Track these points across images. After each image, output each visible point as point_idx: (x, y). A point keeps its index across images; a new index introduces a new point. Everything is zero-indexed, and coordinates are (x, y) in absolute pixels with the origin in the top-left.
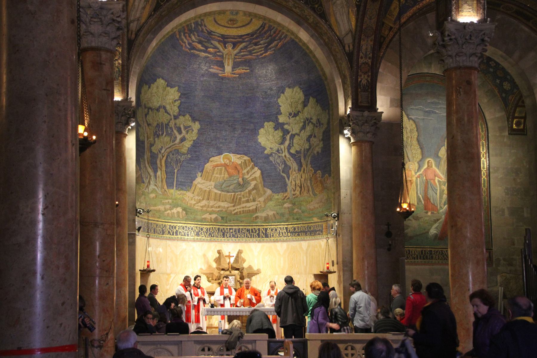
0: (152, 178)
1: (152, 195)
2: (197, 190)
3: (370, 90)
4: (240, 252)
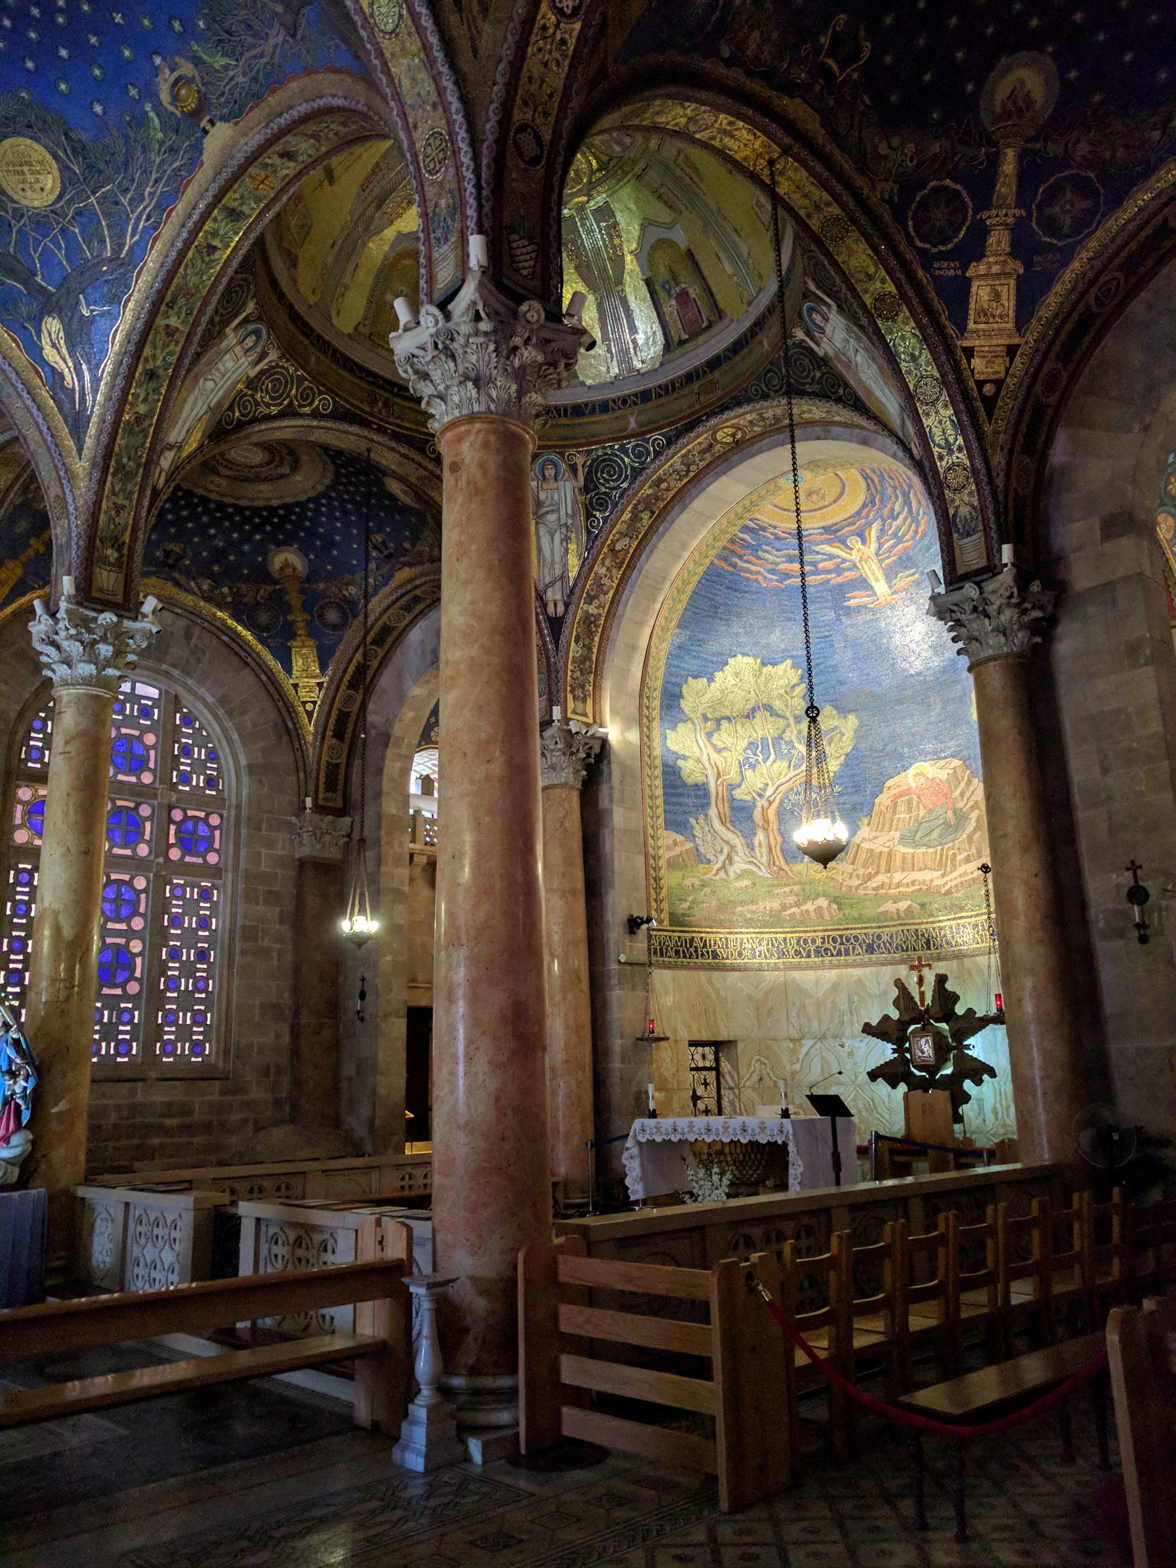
0: (739, 848)
1: (746, 882)
2: (862, 856)
3: (981, 527)
4: (941, 980)
